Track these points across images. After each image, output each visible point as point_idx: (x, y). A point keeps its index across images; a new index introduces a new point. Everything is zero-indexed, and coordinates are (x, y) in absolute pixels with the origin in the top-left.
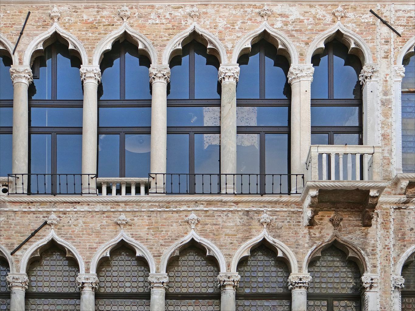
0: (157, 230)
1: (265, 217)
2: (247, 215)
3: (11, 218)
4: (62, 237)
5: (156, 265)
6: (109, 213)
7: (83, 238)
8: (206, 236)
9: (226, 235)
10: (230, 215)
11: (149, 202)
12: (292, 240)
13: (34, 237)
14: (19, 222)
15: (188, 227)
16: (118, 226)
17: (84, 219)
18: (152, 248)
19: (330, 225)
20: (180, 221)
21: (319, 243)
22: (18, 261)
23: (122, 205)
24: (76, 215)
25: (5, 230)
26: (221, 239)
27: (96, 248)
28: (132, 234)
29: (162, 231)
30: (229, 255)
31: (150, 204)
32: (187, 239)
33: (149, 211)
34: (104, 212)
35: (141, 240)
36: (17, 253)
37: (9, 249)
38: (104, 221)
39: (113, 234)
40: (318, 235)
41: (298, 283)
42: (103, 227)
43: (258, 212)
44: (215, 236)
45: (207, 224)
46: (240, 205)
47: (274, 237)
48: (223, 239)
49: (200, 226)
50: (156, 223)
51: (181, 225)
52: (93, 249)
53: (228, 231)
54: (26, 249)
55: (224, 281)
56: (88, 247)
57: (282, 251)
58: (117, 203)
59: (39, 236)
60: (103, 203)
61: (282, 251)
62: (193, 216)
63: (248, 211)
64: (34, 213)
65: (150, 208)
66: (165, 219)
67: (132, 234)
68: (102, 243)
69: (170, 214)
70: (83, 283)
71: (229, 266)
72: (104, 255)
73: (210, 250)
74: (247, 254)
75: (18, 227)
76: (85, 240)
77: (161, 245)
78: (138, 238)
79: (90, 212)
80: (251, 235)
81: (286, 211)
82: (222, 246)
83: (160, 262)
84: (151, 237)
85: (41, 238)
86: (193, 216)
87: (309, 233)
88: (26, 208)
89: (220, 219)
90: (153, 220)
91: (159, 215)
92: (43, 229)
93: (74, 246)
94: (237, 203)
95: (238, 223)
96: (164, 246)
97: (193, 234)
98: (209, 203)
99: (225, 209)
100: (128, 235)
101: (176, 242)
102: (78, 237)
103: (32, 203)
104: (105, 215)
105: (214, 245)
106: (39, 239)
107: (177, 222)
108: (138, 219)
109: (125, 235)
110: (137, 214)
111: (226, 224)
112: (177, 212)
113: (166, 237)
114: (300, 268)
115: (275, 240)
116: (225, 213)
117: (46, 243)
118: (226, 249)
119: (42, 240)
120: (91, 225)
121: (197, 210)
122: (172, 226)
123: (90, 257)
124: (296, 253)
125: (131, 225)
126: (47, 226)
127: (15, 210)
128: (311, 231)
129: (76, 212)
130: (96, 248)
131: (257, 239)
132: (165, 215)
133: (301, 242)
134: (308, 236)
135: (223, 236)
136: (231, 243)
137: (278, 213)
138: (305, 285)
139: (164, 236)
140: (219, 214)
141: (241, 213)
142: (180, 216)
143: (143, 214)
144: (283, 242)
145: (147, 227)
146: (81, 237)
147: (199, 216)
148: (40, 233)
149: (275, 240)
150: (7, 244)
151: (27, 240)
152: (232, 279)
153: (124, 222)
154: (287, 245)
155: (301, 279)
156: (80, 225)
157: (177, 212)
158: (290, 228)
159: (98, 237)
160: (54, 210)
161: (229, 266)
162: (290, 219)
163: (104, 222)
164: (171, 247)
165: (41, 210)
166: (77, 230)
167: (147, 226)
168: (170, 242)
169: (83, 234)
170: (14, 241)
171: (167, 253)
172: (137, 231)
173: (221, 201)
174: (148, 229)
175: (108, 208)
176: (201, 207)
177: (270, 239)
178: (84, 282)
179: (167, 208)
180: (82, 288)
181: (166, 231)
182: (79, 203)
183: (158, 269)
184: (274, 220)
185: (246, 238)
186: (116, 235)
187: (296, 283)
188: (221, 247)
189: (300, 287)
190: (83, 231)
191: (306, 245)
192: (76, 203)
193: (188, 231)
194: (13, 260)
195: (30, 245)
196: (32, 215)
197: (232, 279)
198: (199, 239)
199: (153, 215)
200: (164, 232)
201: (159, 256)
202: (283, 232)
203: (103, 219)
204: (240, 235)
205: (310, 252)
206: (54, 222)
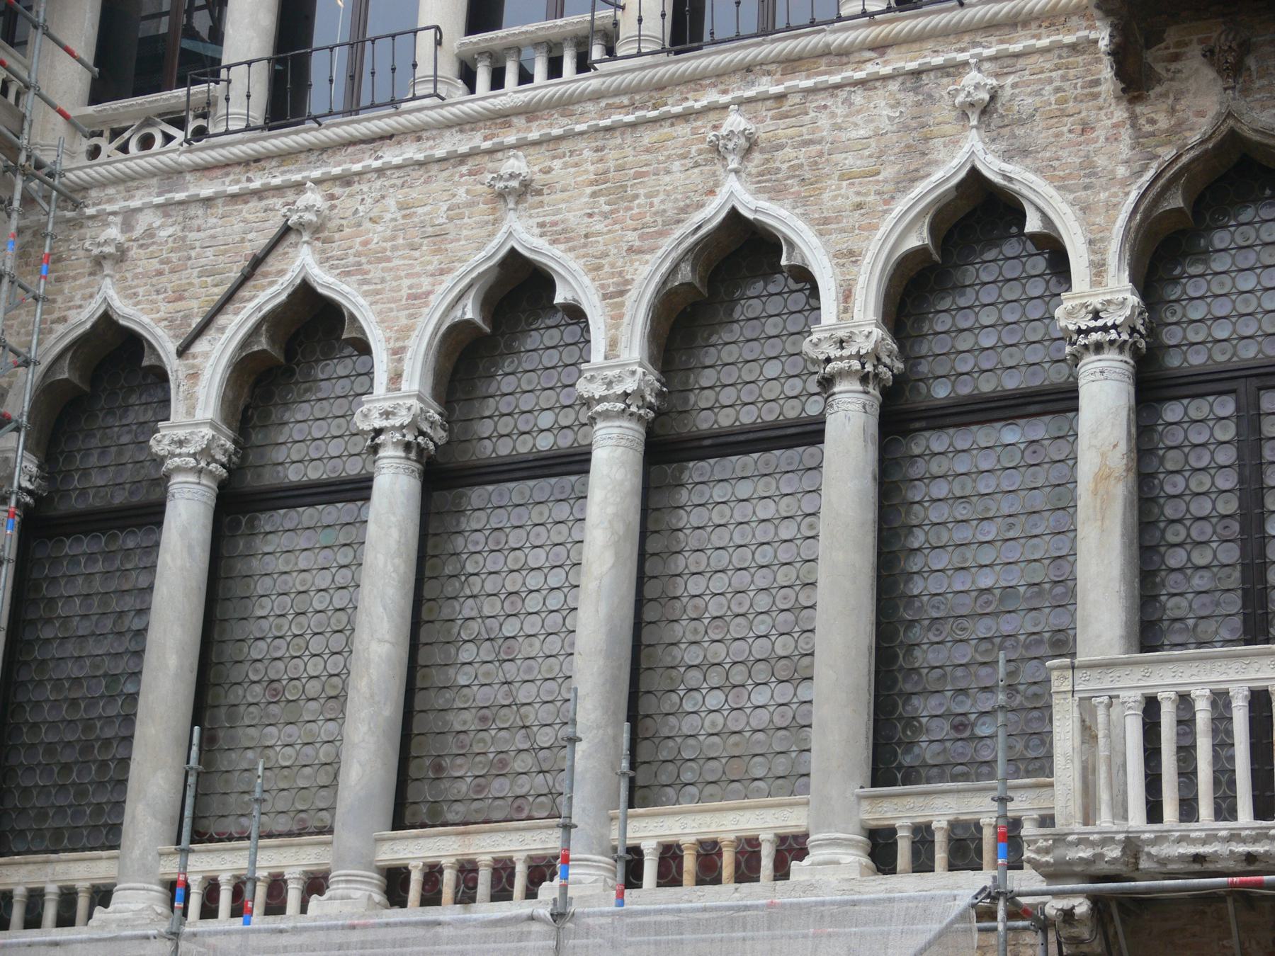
0: (621, 195)
1: (974, 83)
2: (915, 90)
3: (196, 223)
4: (332, 267)
5: (609, 327)
6: (478, 160)
7: (395, 262)
8: (776, 193)
9: (841, 178)
10: (858, 98)
11: (596, 96)
12: (1071, 159)
13: (251, 283)
14: (213, 237)
15: (718, 167)
16: (501, 205)
17: (400, 195)
18: (598, 268)
19: (1209, 74)
20: (694, 149)
21: (1167, 153)
22: (194, 376)
23: (519, 122)
24: (379, 183)
25: (173, 271)
26: (826, 196)
27: (428, 294)
28: (542, 225)
29: (636, 196)
30: (851, 253)
31: (603, 103)
32: (711, 213)
33: (597, 130)
34: (463, 158)
35: (568, 240)
36: (200, 347)
37: (176, 337)
38: (461, 191)
39: (483, 232)
40: (1163, 122)
41: (1087, 332)
42: (455, 212)
43: (953, 70)
44: (803, 186)
45: (782, 147)
46: (891, 54)
47: (1008, 156)
48: (837, 195)
49: (757, 157)
50: (620, 169)
51: (697, 165)
52: (419, 298)
53: (850, 161)
54: (222, 330)
55: (828, 360)
56: (405, 292)
57: (1038, 209)
58: (502, 117)
59: (265, 275)
60: (463, 124)
61: (1038, 209)
62: (735, 121)
63: (917, 73)
64: (259, 194)
65: (602, 117)
66: (648, 151)
67: (542, 225)
68: (450, 271)
69: (666, 130)
70: (378, 432)
71: (847, 295)
72: (457, 315)
73: (791, 245)
74: (918, 239)
75: (209, 252)
76: (397, 268)
77: (631, 250)
78: (558, 234)
79: (421, 164)
80: (929, 164)
81: (1046, 50)
82: (826, 221)
83: (621, 316)
84: (600, 227)
85: (272, 283)
86: (735, 121)
87: (1133, 118)
88: (238, 182)
89: (824, 121)
90: (612, 156)
91: (629, 140)
92: (280, 250)
93: (365, 294)
94: (880, 48)
95: (885, 125)
96: (640, 251)
97: (739, 193)
98: (791, 64)
99: (836, 79)
100: (528, 229)
101: (678, 232)
102: (380, 260)
103: (257, 161)
104: (464, 169)
105: (801, 225)
106: (263, 288)
107: (684, 157)
108: (565, 166)
109: (524, 233)
110: (565, 146)
111: (843, 136)
112: (685, 116)
113: (648, 219)
114: (1098, 269)
115: (1008, 168)
116: (843, 94)
117: (283, 297)
118: (843, 230)
119: (275, 288)
120: (420, 210)
121: (750, 100)
122: (668, 172)
123: (405, 332)
124: (1085, 209)
125: (539, 193)
126: (292, 238)
127: (206, 191)
128: (1139, 109)
129: (380, 172)
130: (428, 294)
131: (945, 172)
132: (648, 137)
133: (1101, 161)
134: (1126, 134)
135: (833, 182)
136: (859, 206)
137: (1021, 63)
138: (1113, 335)
139: (641, 216)
140: (821, 100)
141: (894, 86)
142: (694, 132)
143: (582, 144)
144: (1037, 171)
145: (589, 190)
146: (388, 260)
147: (754, 118)
148: (272, 264)
149: (1008, 168)
150: (172, 321)
151: (229, 298)
152: (851, 349)
153: (514, 184)
154: (1051, 180)
155: (1096, 315)
156: (388, 216)
157: (685, 116)
158: (1064, 114)
159: (438, 251)
160: (317, 174)
161: (847, 295)
162: (1064, 78)
163: (462, 195)
164: (660, 253)
165: (277, 181)
166: (376, 235)
167: (591, 184)
168: (661, 234)
169: (394, 248)
170: (194, 304)
171: (646, 276)
172: (558, 212)
173: (826, 52)
174: (594, 195)
175: (477, 140)
176: (768, 86)
177: (993, 168)
178: (378, 424)
179: (655, 108)
180: (375, 449)
181: (648, 196)
182: (391, 137)
183: (613, 344)
184: (1008, 91)
185: (913, 178)
186: (491, 235)
187: (1079, 331)
188: (823, 225)
189: (1099, 347)
190: (394, 238)
191: (1122, 171)
192: (382, 138)
193: (717, 184)
194: (181, 375)
195: (236, 314)
196: (254, 204)
197: (851, 349)
198: (753, 205)
199: (612, 143)
200: (641, 200)
201: (622, 293)
202: (1038, 134)
203: (457, 184)
204: (888, 172)
205: (1133, 196)
206: (309, 217)
